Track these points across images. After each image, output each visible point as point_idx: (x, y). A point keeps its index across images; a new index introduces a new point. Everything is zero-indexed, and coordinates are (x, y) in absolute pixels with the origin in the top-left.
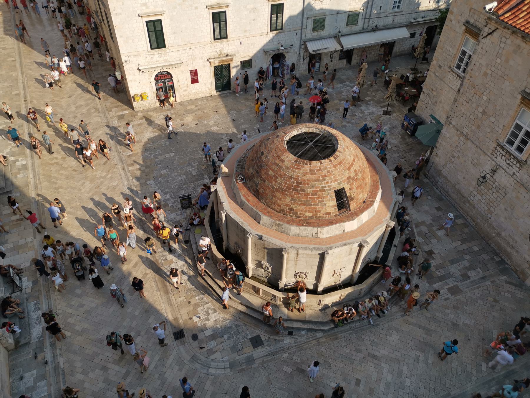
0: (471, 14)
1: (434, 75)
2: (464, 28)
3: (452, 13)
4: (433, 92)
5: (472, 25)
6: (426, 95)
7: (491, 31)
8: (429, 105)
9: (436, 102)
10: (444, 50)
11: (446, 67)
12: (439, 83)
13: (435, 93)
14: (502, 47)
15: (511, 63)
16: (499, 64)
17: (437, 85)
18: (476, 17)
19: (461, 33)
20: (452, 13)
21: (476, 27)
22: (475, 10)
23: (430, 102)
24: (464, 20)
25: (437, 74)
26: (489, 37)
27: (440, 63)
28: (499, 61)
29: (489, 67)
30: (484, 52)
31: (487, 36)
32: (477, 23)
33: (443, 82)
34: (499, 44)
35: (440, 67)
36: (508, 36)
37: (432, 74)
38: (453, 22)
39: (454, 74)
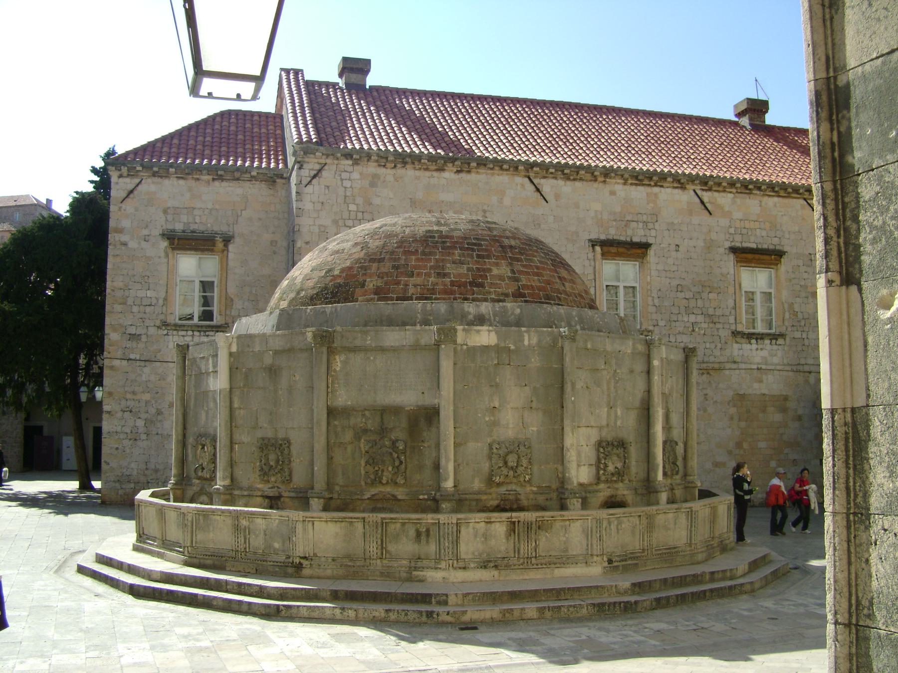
0: (170, 217)
1: (125, 363)
2: (165, 244)
3: (120, 231)
4: (137, 397)
5: (184, 231)
6: (120, 414)
7: (315, 172)
8: (141, 430)
9: (159, 412)
10: (130, 301)
11: (152, 331)
12: (146, 370)
13: (146, 397)
14: (349, 186)
15: (376, 201)
16: (357, 211)
17: (144, 378)
18: (184, 218)
19: (163, 254)
20: (120, 231)
21: (193, 232)
22: (175, 208)
23: (140, 423)
24: (157, 232)
25: (132, 356)
26: (314, 181)
27: (133, 330)
28: (353, 207)
29: (341, 223)
30: (319, 206)
31: (310, 181)
32: (193, 227)
33: (158, 364)
34: (339, 183)
35: (134, 337)
36: (350, 169)
37: (117, 363)
38: (132, 244)
39: (184, 333)
